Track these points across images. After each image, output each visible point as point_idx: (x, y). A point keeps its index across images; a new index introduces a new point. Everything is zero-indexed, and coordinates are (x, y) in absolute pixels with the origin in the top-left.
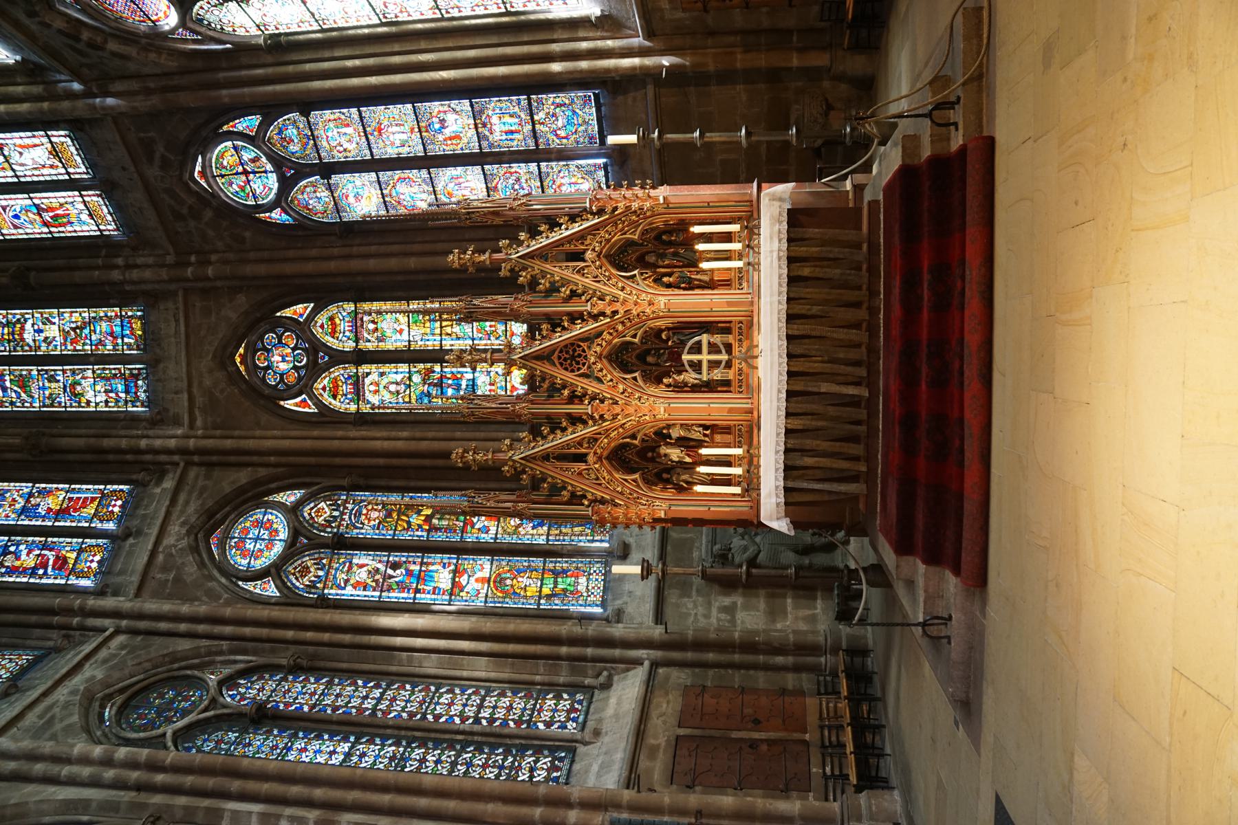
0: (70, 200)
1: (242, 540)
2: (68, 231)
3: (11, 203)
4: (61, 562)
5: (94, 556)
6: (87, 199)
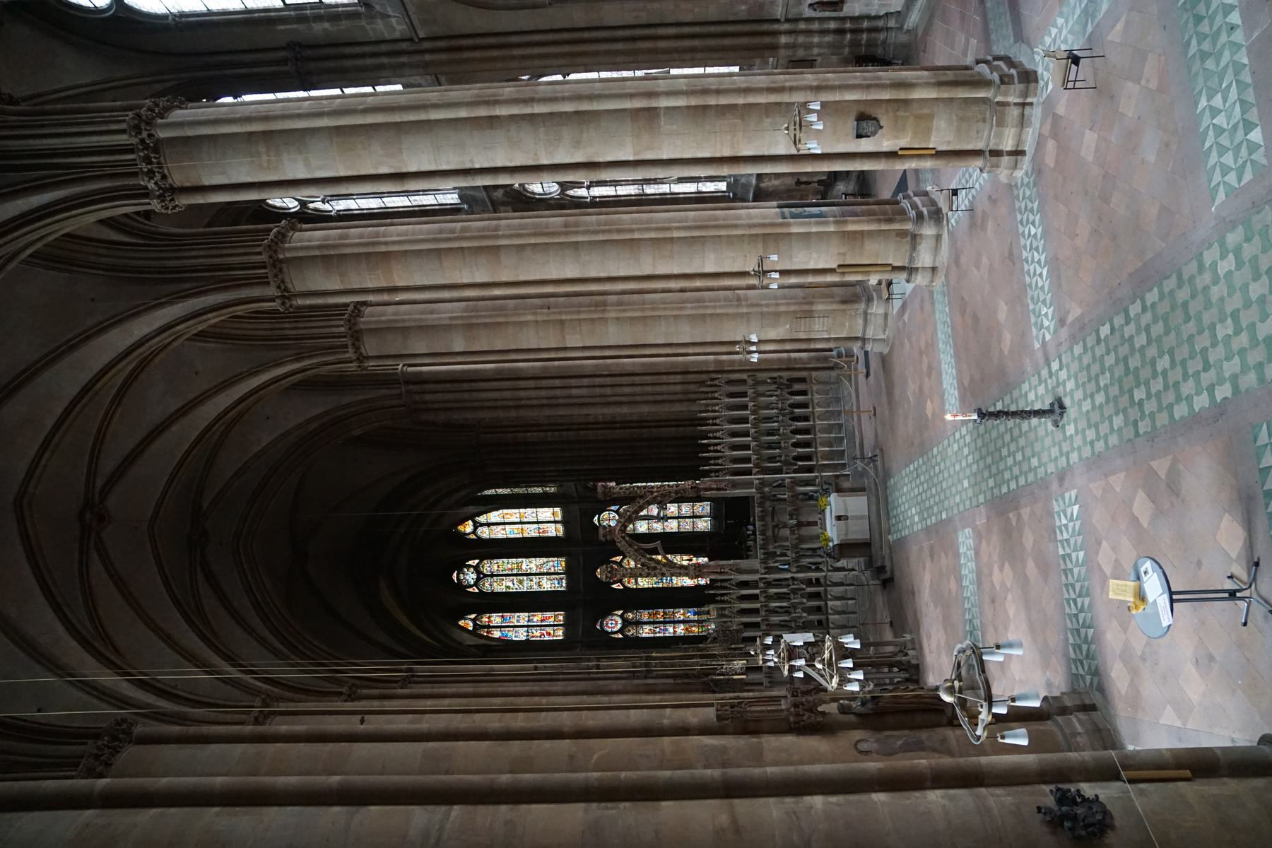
1: (607, 624)
4: (549, 634)
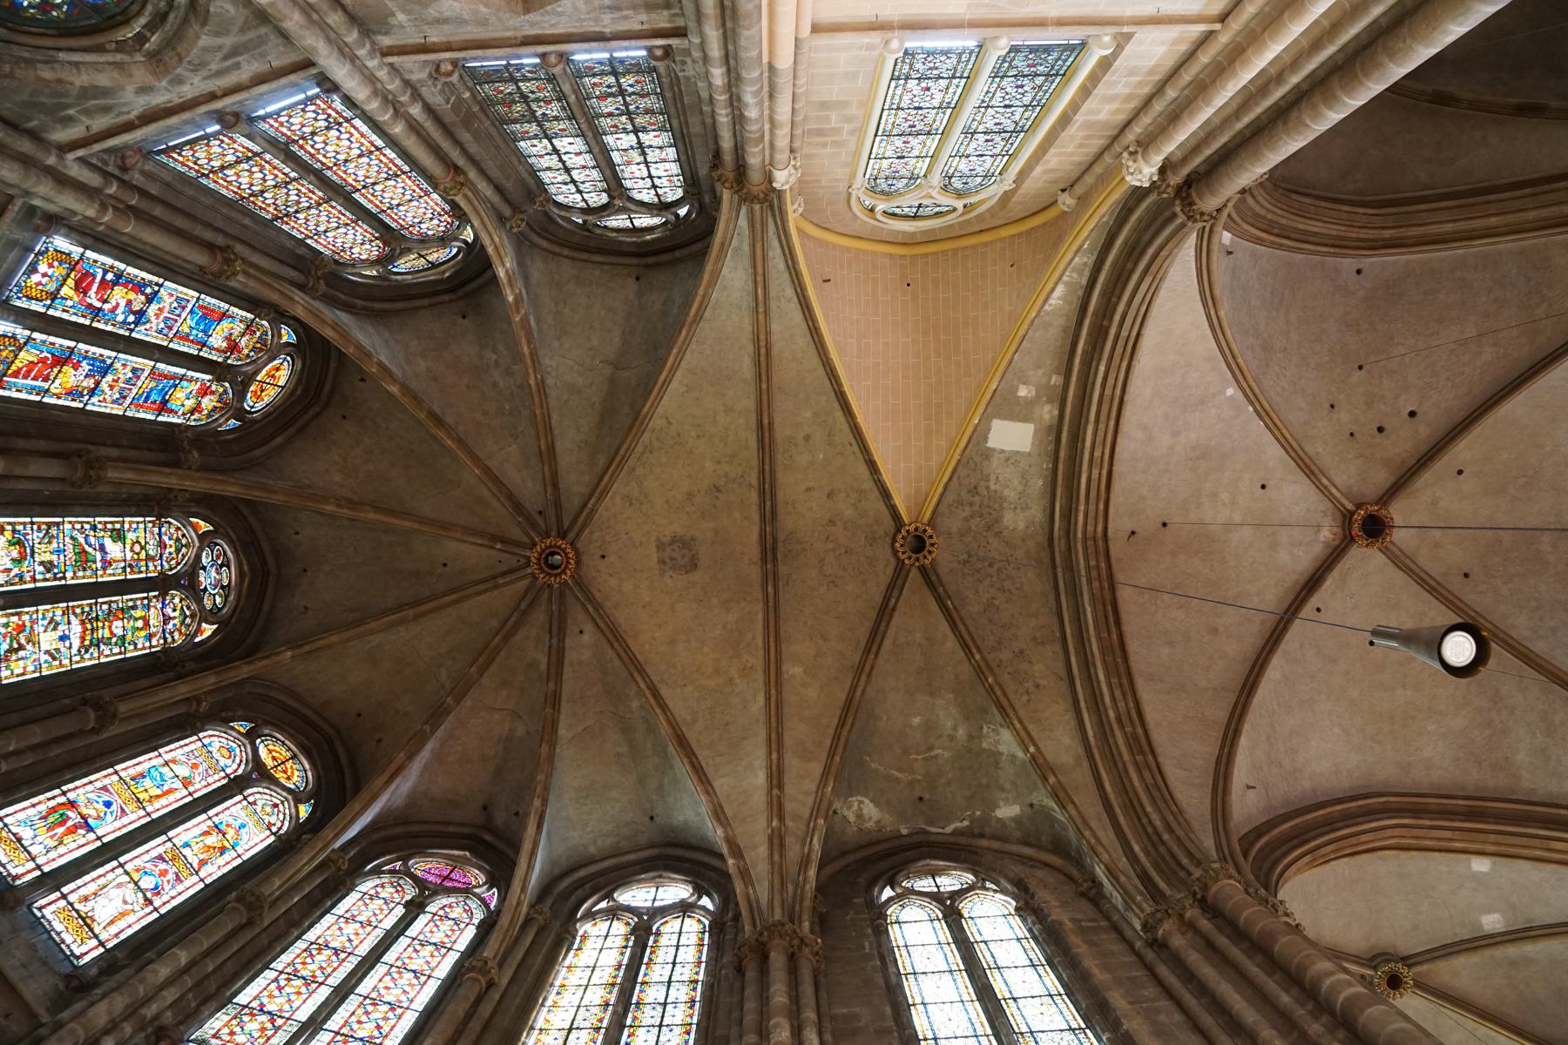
0: (52, 855)
2: (44, 802)
3: (118, 824)
5: (39, 283)
6: (31, 865)
